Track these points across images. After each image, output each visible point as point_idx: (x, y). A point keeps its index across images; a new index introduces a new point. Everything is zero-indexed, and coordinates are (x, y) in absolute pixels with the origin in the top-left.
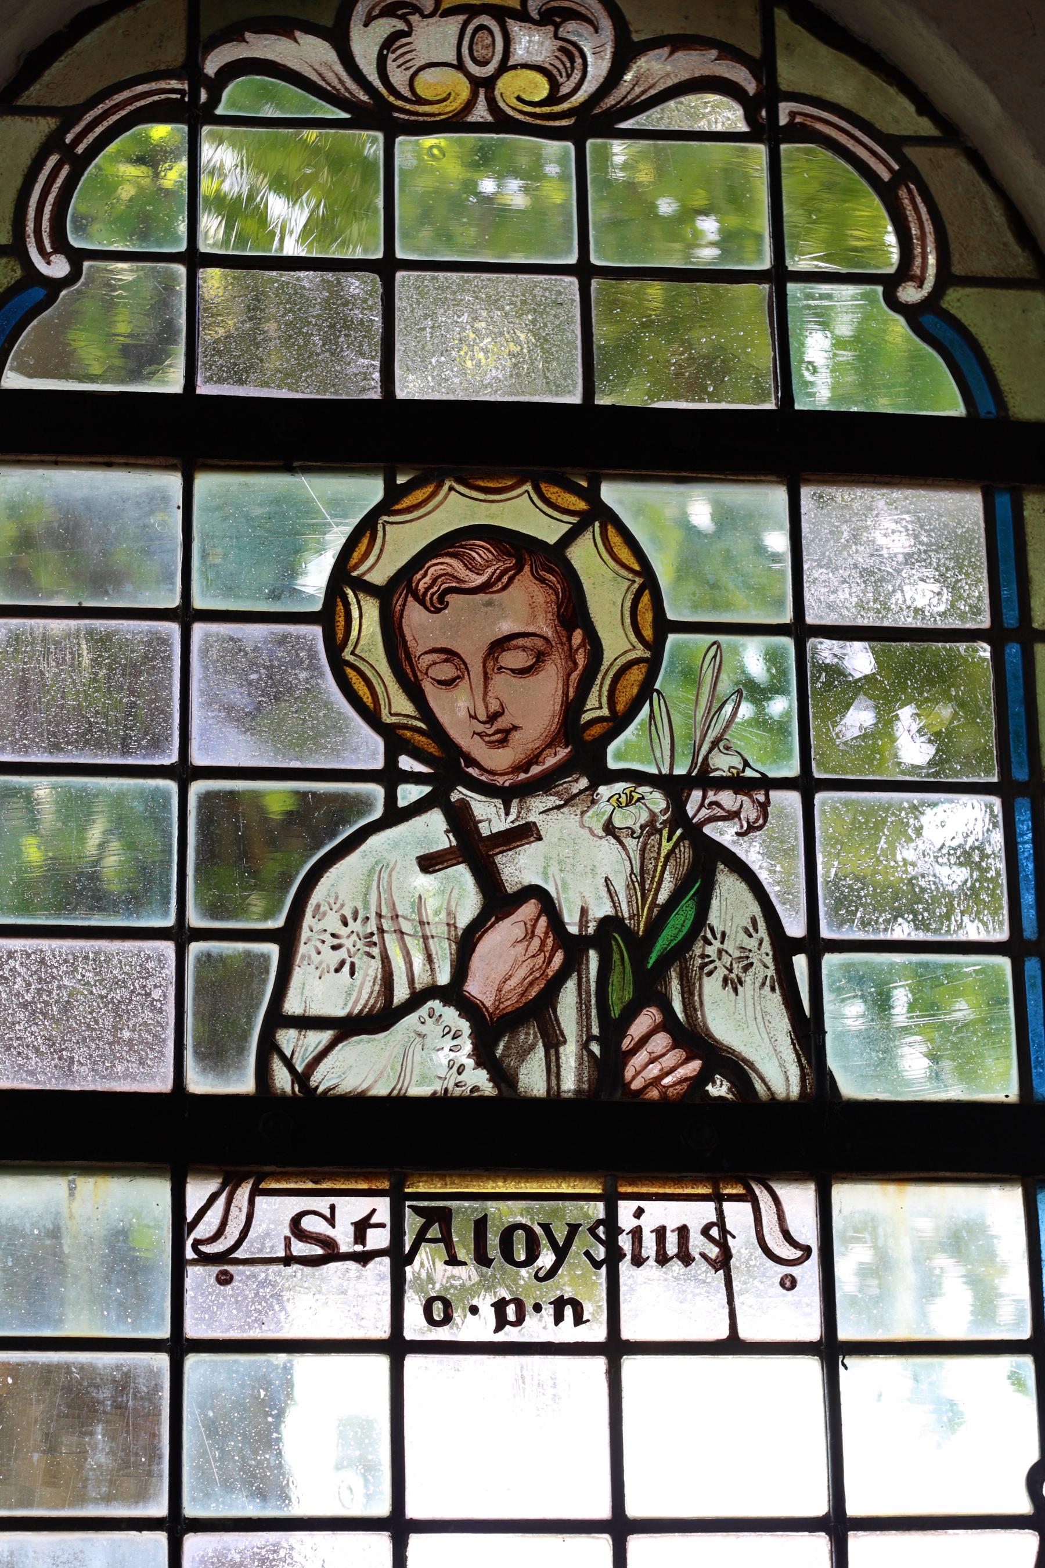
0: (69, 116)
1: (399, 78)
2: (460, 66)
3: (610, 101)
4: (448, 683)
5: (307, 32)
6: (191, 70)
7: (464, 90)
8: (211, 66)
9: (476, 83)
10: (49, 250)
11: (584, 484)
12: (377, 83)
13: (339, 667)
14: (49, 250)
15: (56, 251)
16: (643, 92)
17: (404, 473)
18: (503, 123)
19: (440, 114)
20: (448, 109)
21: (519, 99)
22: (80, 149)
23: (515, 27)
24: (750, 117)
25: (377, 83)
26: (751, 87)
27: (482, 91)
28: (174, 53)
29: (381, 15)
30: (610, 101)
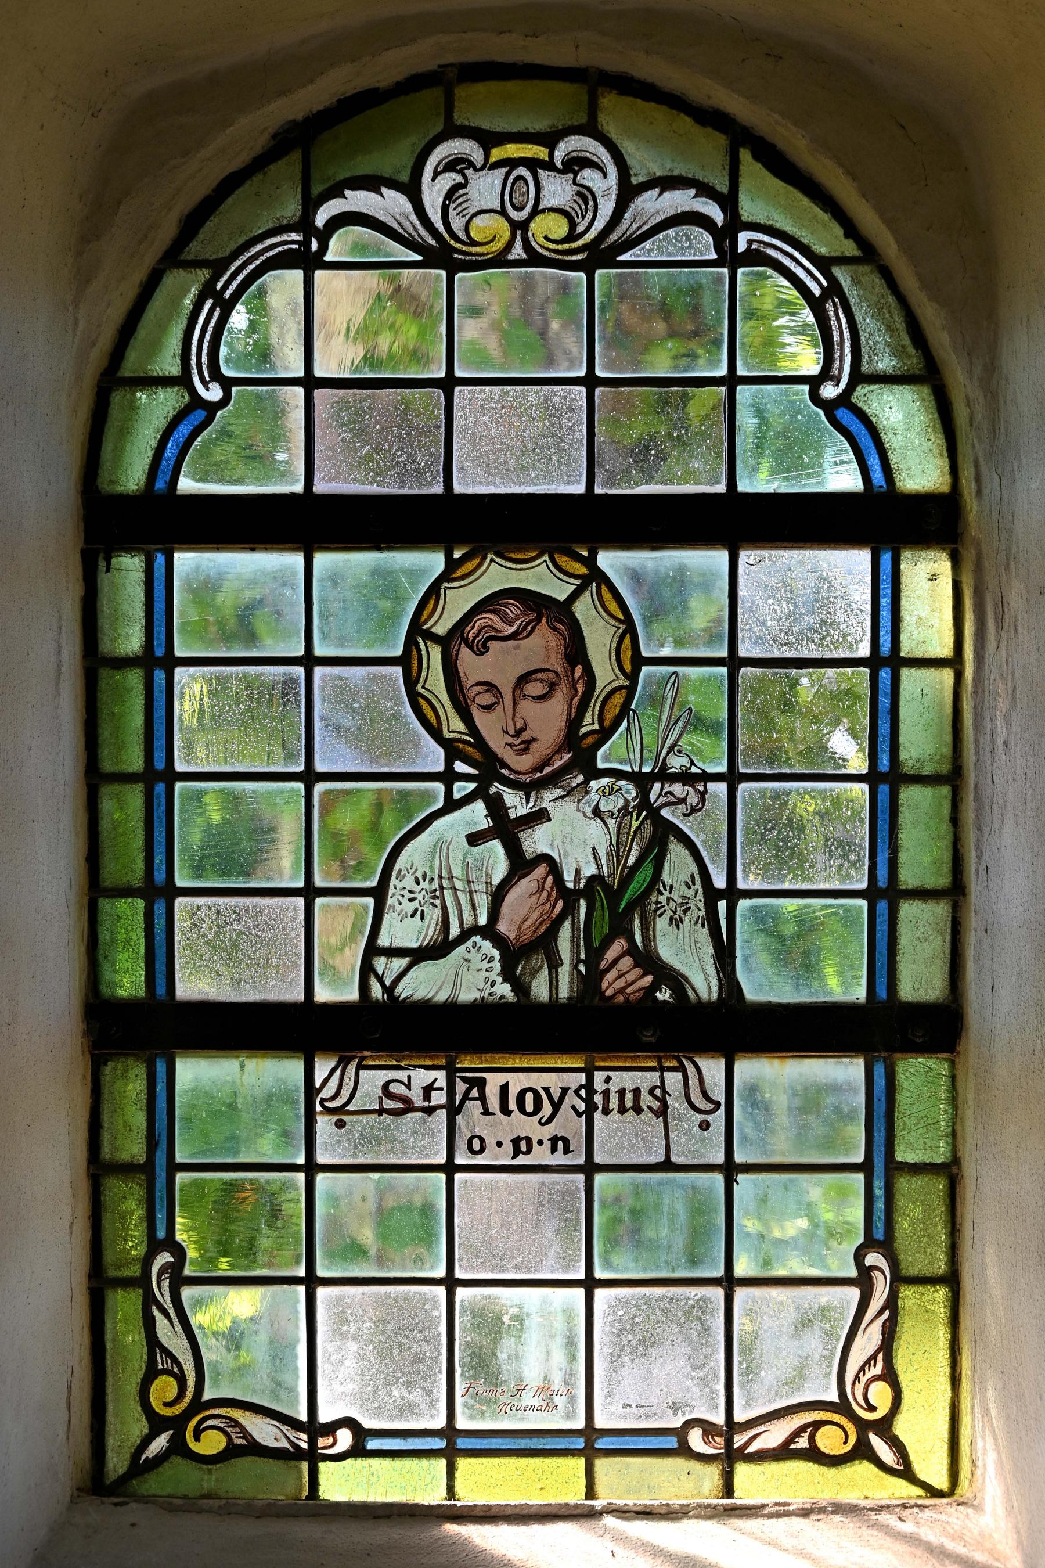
0: (219, 267)
1: (457, 224)
2: (503, 212)
3: (614, 237)
4: (488, 708)
5: (389, 188)
6: (305, 224)
7: (504, 230)
8: (321, 218)
9: (515, 225)
10: (208, 379)
11: (585, 554)
12: (441, 228)
13: (414, 697)
14: (208, 379)
15: (213, 379)
16: (639, 228)
17: (459, 549)
18: (534, 259)
19: (488, 254)
20: (493, 249)
21: (546, 238)
22: (227, 294)
23: (543, 174)
24: (718, 248)
25: (441, 228)
26: (718, 216)
27: (519, 233)
28: (292, 209)
29: (445, 170)
30: (614, 237)
